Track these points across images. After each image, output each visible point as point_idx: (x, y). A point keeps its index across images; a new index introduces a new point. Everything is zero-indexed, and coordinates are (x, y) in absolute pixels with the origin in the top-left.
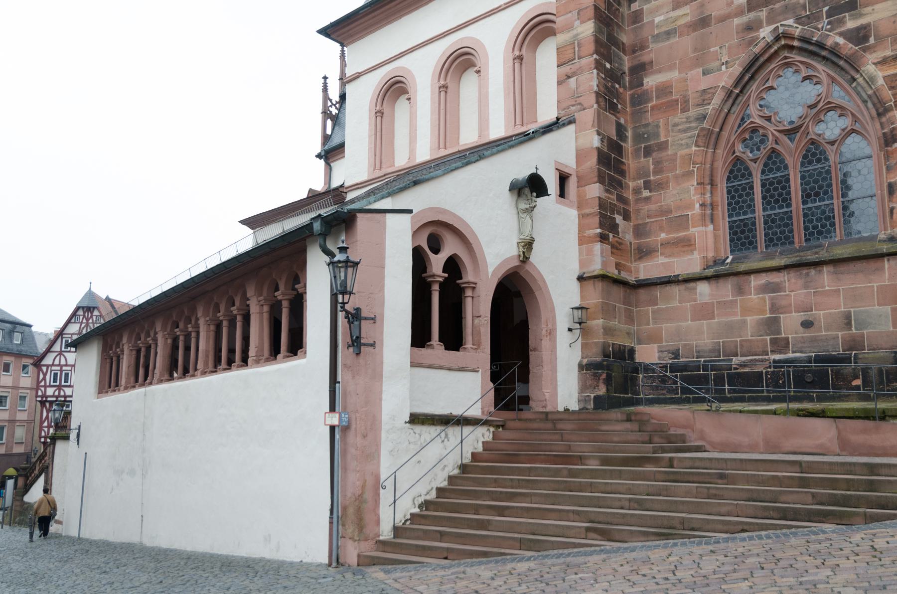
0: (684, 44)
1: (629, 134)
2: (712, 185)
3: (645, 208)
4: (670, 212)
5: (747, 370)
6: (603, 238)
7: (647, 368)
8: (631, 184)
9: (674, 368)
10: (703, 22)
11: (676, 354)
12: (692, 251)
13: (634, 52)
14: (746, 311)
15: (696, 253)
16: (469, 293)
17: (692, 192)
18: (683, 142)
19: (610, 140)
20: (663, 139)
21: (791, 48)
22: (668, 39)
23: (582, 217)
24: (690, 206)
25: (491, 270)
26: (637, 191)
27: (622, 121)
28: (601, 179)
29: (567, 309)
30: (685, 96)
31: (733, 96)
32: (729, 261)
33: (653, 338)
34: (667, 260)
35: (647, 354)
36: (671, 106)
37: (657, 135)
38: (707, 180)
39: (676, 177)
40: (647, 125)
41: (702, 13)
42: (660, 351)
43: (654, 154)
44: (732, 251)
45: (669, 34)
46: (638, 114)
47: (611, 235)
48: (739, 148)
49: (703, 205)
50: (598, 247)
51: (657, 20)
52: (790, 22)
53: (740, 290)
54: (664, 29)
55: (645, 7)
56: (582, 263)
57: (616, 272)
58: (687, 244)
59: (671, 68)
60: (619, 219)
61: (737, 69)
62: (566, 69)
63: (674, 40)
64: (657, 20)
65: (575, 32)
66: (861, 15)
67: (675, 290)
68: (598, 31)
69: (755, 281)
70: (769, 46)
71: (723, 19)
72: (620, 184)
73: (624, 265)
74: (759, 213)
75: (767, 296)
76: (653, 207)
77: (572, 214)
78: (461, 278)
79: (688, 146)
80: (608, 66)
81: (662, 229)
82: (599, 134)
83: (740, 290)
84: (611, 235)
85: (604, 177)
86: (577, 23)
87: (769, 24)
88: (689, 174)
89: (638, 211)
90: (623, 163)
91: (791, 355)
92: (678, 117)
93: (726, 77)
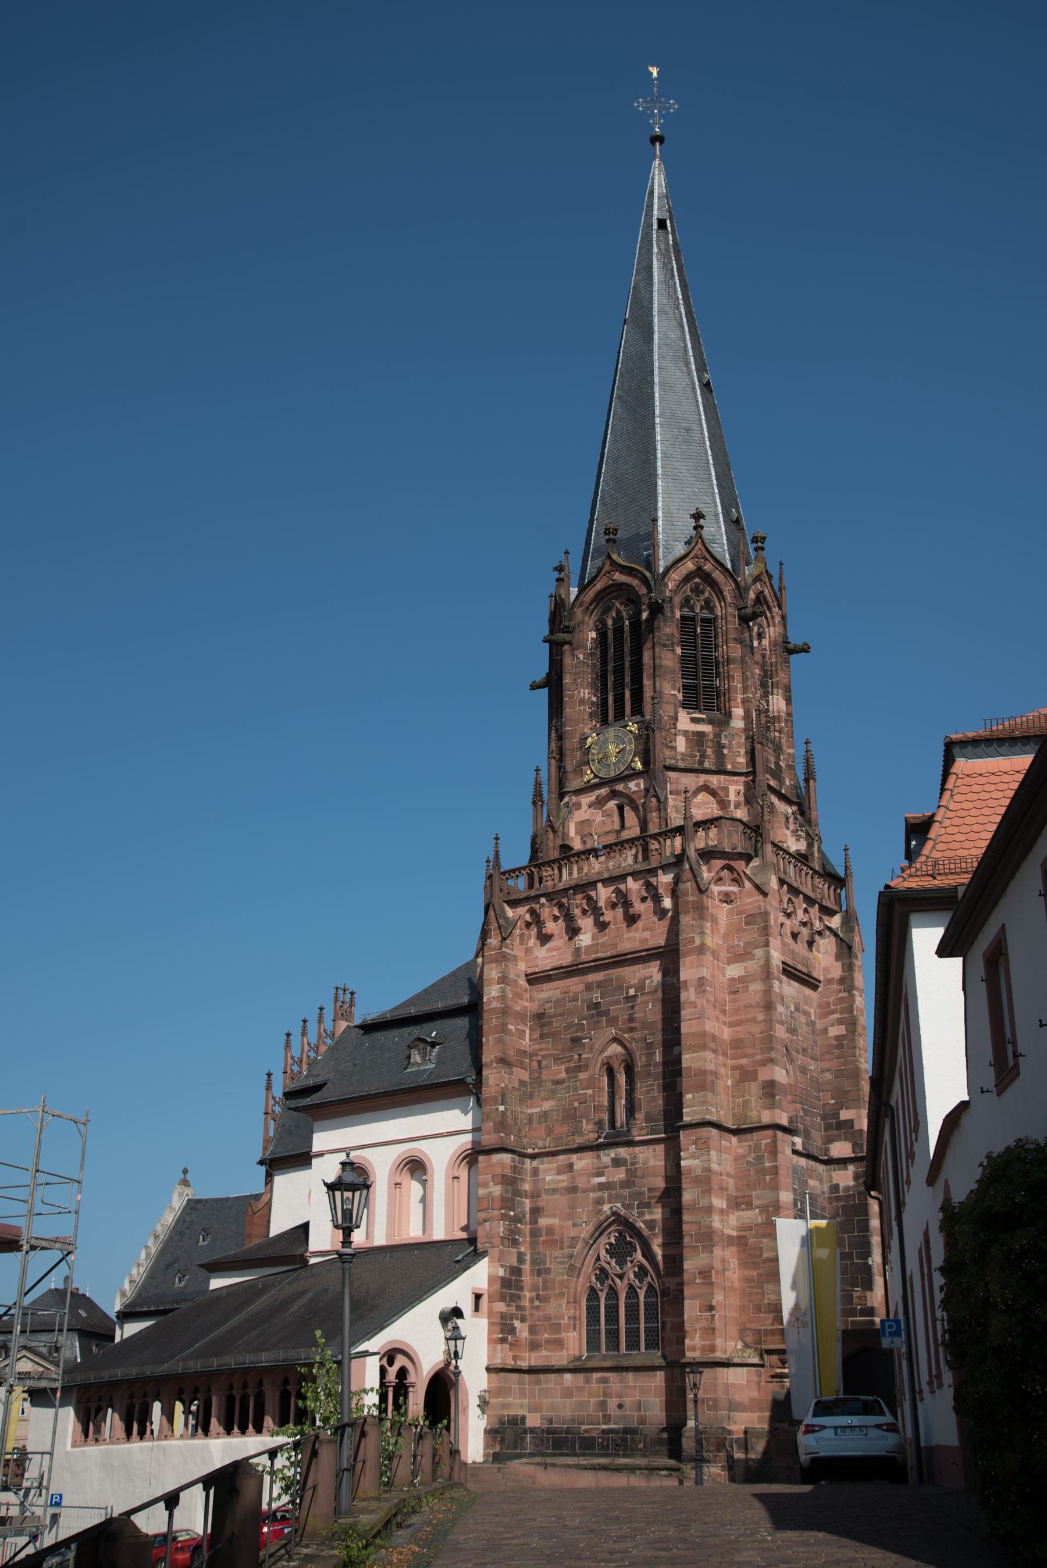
0: (562, 1201)
1: (528, 1258)
3: (537, 1313)
4: (550, 1319)
5: (586, 1435)
6: (503, 1340)
7: (532, 1430)
9: (549, 1431)
10: (573, 1189)
11: (551, 1422)
12: (562, 1350)
13: (533, 1197)
14: (591, 1395)
15: (564, 1351)
16: (411, 1389)
17: (564, 1307)
18: (560, 1271)
20: (548, 1266)
21: (621, 1222)
22: (553, 1194)
23: (490, 1324)
24: (563, 1318)
25: (425, 1373)
27: (523, 1249)
30: (562, 1239)
31: (589, 1245)
32: (584, 1358)
34: (548, 1354)
36: (553, 1243)
37: (545, 1262)
38: (572, 1300)
39: (555, 1295)
40: (539, 1253)
41: (573, 1183)
42: (542, 1419)
43: (543, 1276)
44: (588, 1351)
45: (554, 1191)
47: (510, 1337)
48: (593, 1279)
49: (569, 1318)
51: (548, 1178)
52: (619, 1205)
53: (588, 1381)
54: (552, 1187)
55: (541, 1167)
56: (490, 1357)
57: (513, 1363)
58: (559, 1344)
59: (554, 1216)
60: (517, 1324)
61: (590, 1228)
64: (548, 1178)
65: (490, 1190)
66: (651, 1213)
67: (552, 1376)
71: (585, 1191)
72: (519, 1297)
73: (520, 1356)
75: (601, 1385)
76: (541, 1313)
78: (406, 1379)
79: (563, 1275)
80: (512, 1213)
81: (545, 1331)
82: (502, 1266)
83: (588, 1381)
84: (510, 1337)
85: (506, 1297)
86: (491, 1184)
87: (609, 1203)
88: (562, 1294)
89: (532, 1315)
90: (522, 1281)
91: (612, 1426)
92: (558, 1253)
93: (586, 1231)
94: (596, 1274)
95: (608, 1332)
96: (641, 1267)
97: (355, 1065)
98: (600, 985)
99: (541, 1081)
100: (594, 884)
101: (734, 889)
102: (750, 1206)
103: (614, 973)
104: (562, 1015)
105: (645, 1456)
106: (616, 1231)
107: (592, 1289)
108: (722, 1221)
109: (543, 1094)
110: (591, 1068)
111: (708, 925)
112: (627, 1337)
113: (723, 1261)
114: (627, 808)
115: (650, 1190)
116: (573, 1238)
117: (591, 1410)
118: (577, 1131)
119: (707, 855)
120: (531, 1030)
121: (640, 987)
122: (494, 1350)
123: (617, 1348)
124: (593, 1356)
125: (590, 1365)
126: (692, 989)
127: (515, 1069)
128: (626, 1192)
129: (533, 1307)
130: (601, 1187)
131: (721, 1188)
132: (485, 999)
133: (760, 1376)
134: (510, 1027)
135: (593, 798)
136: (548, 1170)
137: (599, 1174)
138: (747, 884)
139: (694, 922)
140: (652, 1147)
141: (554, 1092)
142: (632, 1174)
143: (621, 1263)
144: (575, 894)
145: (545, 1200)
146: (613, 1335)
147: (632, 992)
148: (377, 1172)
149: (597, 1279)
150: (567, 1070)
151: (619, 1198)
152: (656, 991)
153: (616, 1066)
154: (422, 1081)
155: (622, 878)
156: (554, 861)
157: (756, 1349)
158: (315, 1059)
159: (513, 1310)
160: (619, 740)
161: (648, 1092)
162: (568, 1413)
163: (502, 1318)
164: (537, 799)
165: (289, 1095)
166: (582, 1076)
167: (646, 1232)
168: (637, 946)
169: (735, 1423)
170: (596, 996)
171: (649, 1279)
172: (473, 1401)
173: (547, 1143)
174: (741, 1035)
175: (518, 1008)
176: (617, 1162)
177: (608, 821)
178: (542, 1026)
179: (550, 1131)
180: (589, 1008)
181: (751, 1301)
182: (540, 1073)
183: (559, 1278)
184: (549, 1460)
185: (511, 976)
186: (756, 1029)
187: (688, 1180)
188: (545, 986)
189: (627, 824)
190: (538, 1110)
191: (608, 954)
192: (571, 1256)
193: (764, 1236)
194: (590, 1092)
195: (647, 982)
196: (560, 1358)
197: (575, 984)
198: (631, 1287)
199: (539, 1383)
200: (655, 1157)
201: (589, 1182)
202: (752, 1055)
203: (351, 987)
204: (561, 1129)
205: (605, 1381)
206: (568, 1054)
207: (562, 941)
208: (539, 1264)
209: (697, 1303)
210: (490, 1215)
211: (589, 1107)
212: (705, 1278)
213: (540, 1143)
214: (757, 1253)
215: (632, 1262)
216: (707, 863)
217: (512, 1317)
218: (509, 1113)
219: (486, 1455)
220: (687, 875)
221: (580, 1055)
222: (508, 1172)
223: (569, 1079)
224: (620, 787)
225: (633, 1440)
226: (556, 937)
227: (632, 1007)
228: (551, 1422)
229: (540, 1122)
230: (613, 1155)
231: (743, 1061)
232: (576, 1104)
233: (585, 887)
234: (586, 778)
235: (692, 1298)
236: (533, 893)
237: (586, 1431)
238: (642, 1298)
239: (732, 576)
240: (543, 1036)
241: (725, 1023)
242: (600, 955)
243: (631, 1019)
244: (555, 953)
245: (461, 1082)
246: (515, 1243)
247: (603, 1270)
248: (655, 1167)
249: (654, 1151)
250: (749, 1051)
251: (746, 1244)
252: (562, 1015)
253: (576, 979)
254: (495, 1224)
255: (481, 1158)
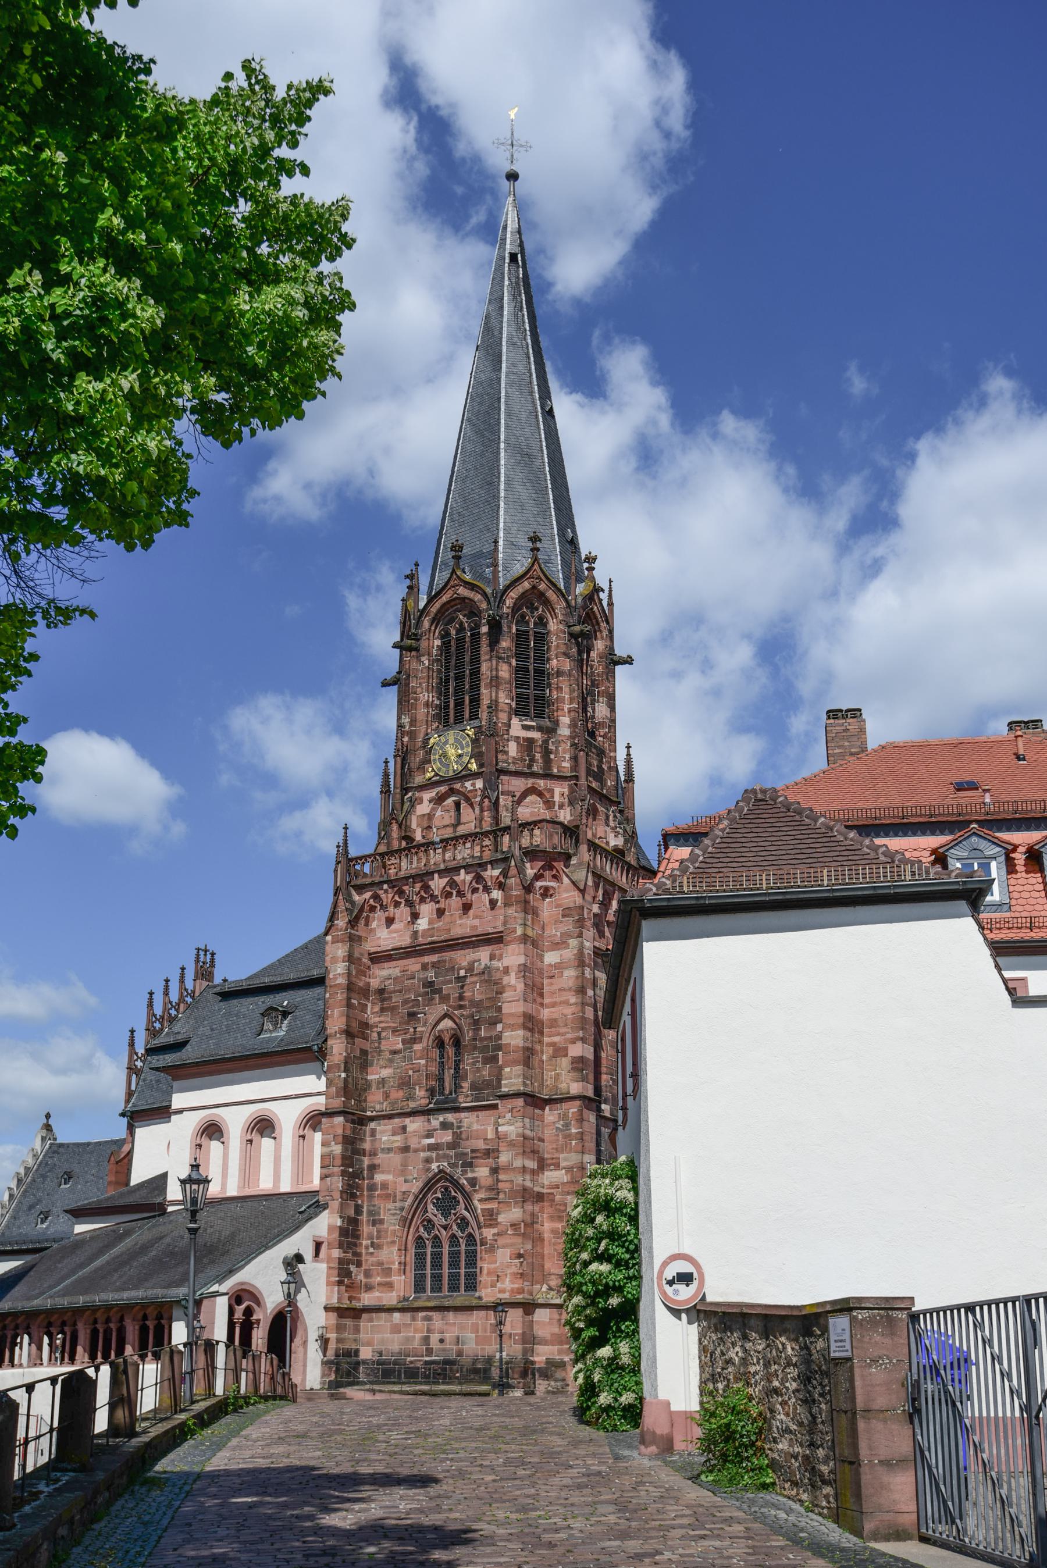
0: (396, 1159)
1: (365, 1209)
2: (405, 1250)
3: (371, 1259)
6: (340, 1283)
7: (364, 1362)
8: (364, 1243)
9: (379, 1363)
10: (406, 1149)
11: (381, 1354)
14: (416, 1331)
19: (349, 1217)
23: (329, 1268)
24: (393, 1263)
26: (367, 1248)
27: (360, 1202)
28: (340, 1246)
29: (316, 1327)
33: (369, 1344)
35: (366, 1353)
36: (388, 1196)
37: (379, 1214)
39: (388, 1243)
40: (374, 1206)
45: (389, 1150)
46: (371, 1197)
48: (421, 1229)
49: (400, 1263)
50: (336, 1288)
51: (384, 1138)
52: (445, 1164)
53: (414, 1319)
56: (328, 1298)
58: (390, 1286)
59: (389, 1172)
60: (352, 1268)
61: (420, 1184)
62: (326, 1171)
63: (391, 1155)
64: (384, 1138)
66: (473, 1171)
68: (345, 1150)
69: (421, 1314)
70: (436, 1175)
71: (416, 1151)
72: (355, 1245)
73: (355, 1298)
74: (428, 1272)
77: (324, 1266)
80: (351, 1170)
81: (378, 1274)
82: (341, 1217)
83: (414, 1319)
88: (394, 1242)
92: (390, 1205)
93: (415, 1187)
94: (424, 1226)
95: (433, 1276)
96: (463, 1219)
97: (212, 1030)
98: (434, 965)
99: (380, 1051)
100: (433, 873)
101: (553, 884)
102: (557, 1166)
103: (447, 955)
104: (400, 991)
105: (460, 1384)
106: (442, 1187)
107: (420, 1237)
108: (532, 1181)
109: (381, 1062)
110: (425, 1040)
111: (530, 917)
112: (450, 1280)
113: (533, 1215)
114: (463, 804)
115: (473, 1151)
116: (404, 1193)
117: (416, 1344)
118: (411, 1097)
119: (532, 854)
120: (373, 1004)
121: (470, 969)
122: (332, 1291)
123: (440, 1290)
124: (419, 1298)
125: (416, 1304)
126: (513, 975)
127: (357, 1040)
128: (452, 1153)
129: (367, 1253)
130: (431, 1148)
131: (533, 1152)
132: (331, 976)
133: (560, 1314)
134: (353, 1001)
135: (433, 794)
136: (383, 1132)
137: (429, 1136)
138: (566, 880)
139: (516, 915)
140: (476, 1113)
141: (391, 1061)
142: (457, 1136)
143: (446, 1215)
144: (414, 883)
145: (381, 1159)
146: (437, 1278)
147: (462, 973)
148: (231, 1130)
149: (425, 1229)
150: (404, 1042)
151: (446, 1157)
152: (483, 973)
153: (447, 1040)
154: (272, 1047)
155: (456, 870)
156: (396, 851)
157: (559, 1291)
158: (176, 1016)
159: (349, 1255)
160: (458, 744)
161: (474, 1064)
162: (395, 1347)
163: (339, 1263)
164: (385, 790)
165: (150, 1051)
166: (417, 1047)
167: (468, 1188)
168: (468, 931)
169: (538, 1354)
170: (430, 975)
171: (470, 1230)
172: (313, 1335)
173: (385, 1107)
174: (555, 1016)
175: (361, 984)
176: (445, 1126)
177: (447, 816)
178: (383, 1000)
179: (387, 1096)
180: (424, 986)
181: (555, 1250)
182: (380, 1043)
183: (392, 1228)
184: (376, 1387)
185: (356, 954)
186: (568, 1011)
187: (504, 1144)
188: (386, 965)
189: (463, 819)
190: (377, 1077)
191: (443, 938)
192: (402, 1209)
193: (568, 1193)
194: (423, 1062)
195: (476, 964)
196: (390, 1298)
197: (413, 965)
198: (454, 1236)
199: (371, 1320)
200: (477, 1121)
201: (420, 1143)
202: (564, 1034)
203: (210, 948)
204: (397, 1095)
205: (428, 1319)
206: (405, 1027)
207: (402, 924)
208: (374, 1215)
209: (508, 1252)
210: (330, 1171)
211: (422, 1075)
212: (515, 1230)
213: (378, 1107)
214: (562, 1208)
215: (455, 1214)
216: (531, 861)
217: (349, 1262)
218: (350, 1080)
219: (323, 1383)
220: (513, 871)
221: (415, 1028)
222: (348, 1132)
223: (405, 1049)
224: (457, 786)
225: (451, 1370)
226: (397, 920)
227: (462, 987)
228: (381, 1354)
229: (378, 1088)
230: (441, 1119)
231: (556, 1039)
232: (411, 1073)
233: (423, 877)
234: (428, 775)
235: (504, 1247)
236: (377, 879)
237: (411, 1362)
238: (463, 1247)
239: (563, 596)
240: (382, 1010)
241: (542, 1005)
242: (435, 938)
243: (461, 998)
244: (395, 935)
245: (309, 1049)
246: (353, 1197)
247: (430, 1221)
248: (477, 1130)
249: (478, 1116)
250: (562, 1030)
251: (553, 1201)
252: (400, 991)
253: (413, 960)
254: (335, 1179)
255: (324, 1120)
